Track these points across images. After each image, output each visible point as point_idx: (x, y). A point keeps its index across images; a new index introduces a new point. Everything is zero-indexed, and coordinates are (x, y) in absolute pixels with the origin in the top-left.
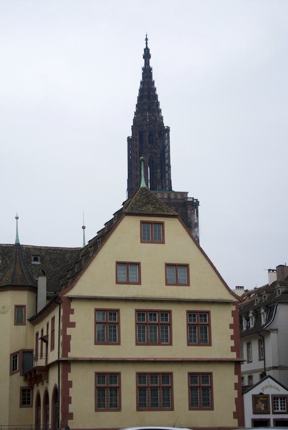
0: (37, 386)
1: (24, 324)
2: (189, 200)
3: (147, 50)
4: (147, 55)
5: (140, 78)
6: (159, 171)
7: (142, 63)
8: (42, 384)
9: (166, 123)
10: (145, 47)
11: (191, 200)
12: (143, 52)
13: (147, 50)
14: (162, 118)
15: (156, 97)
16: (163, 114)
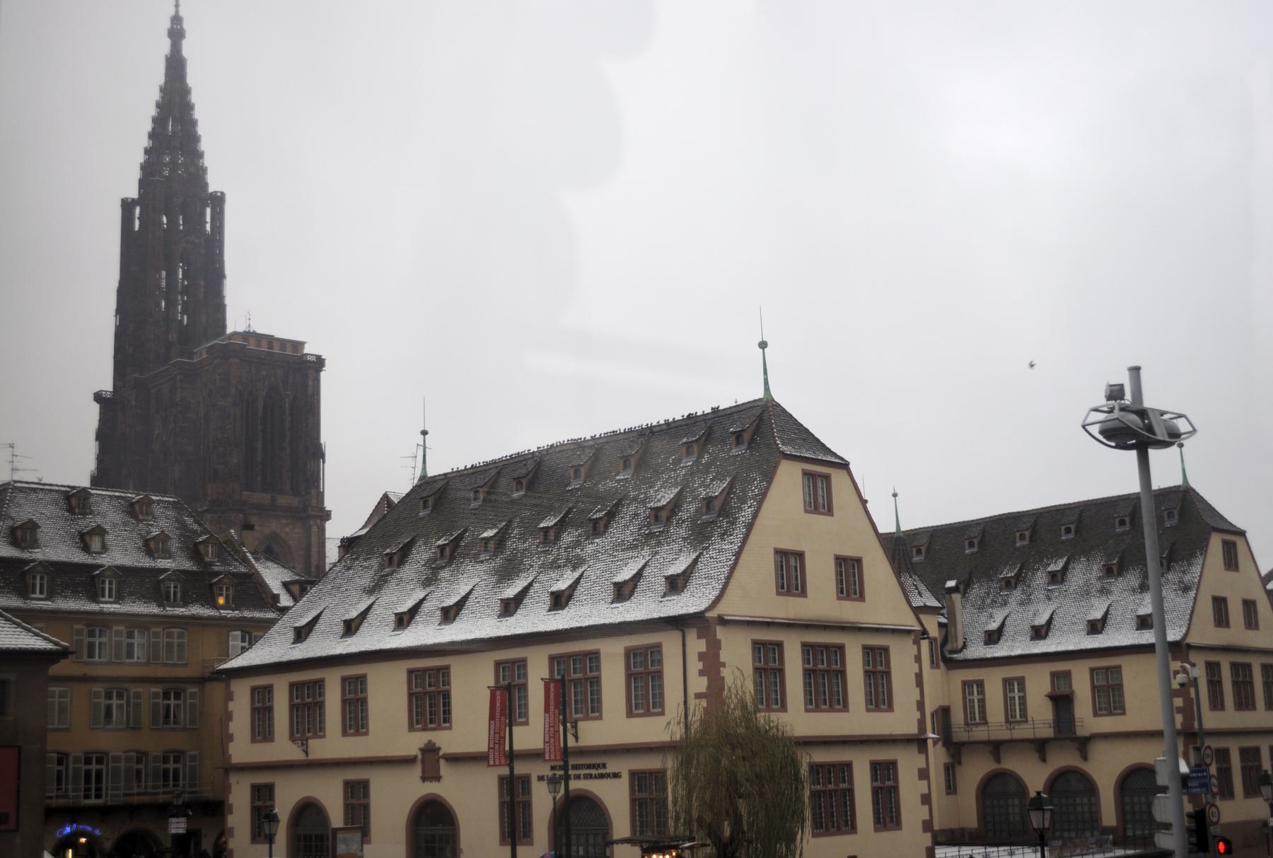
0: (998, 761)
1: (938, 667)
2: (309, 358)
3: (176, 19)
4: (176, 33)
5: (160, 79)
6: (202, 283)
7: (165, 46)
8: (1043, 759)
9: (214, 184)
10: (173, 13)
11: (314, 359)
12: (168, 25)
13: (176, 19)
14: (204, 170)
15: (194, 123)
16: (208, 161)
